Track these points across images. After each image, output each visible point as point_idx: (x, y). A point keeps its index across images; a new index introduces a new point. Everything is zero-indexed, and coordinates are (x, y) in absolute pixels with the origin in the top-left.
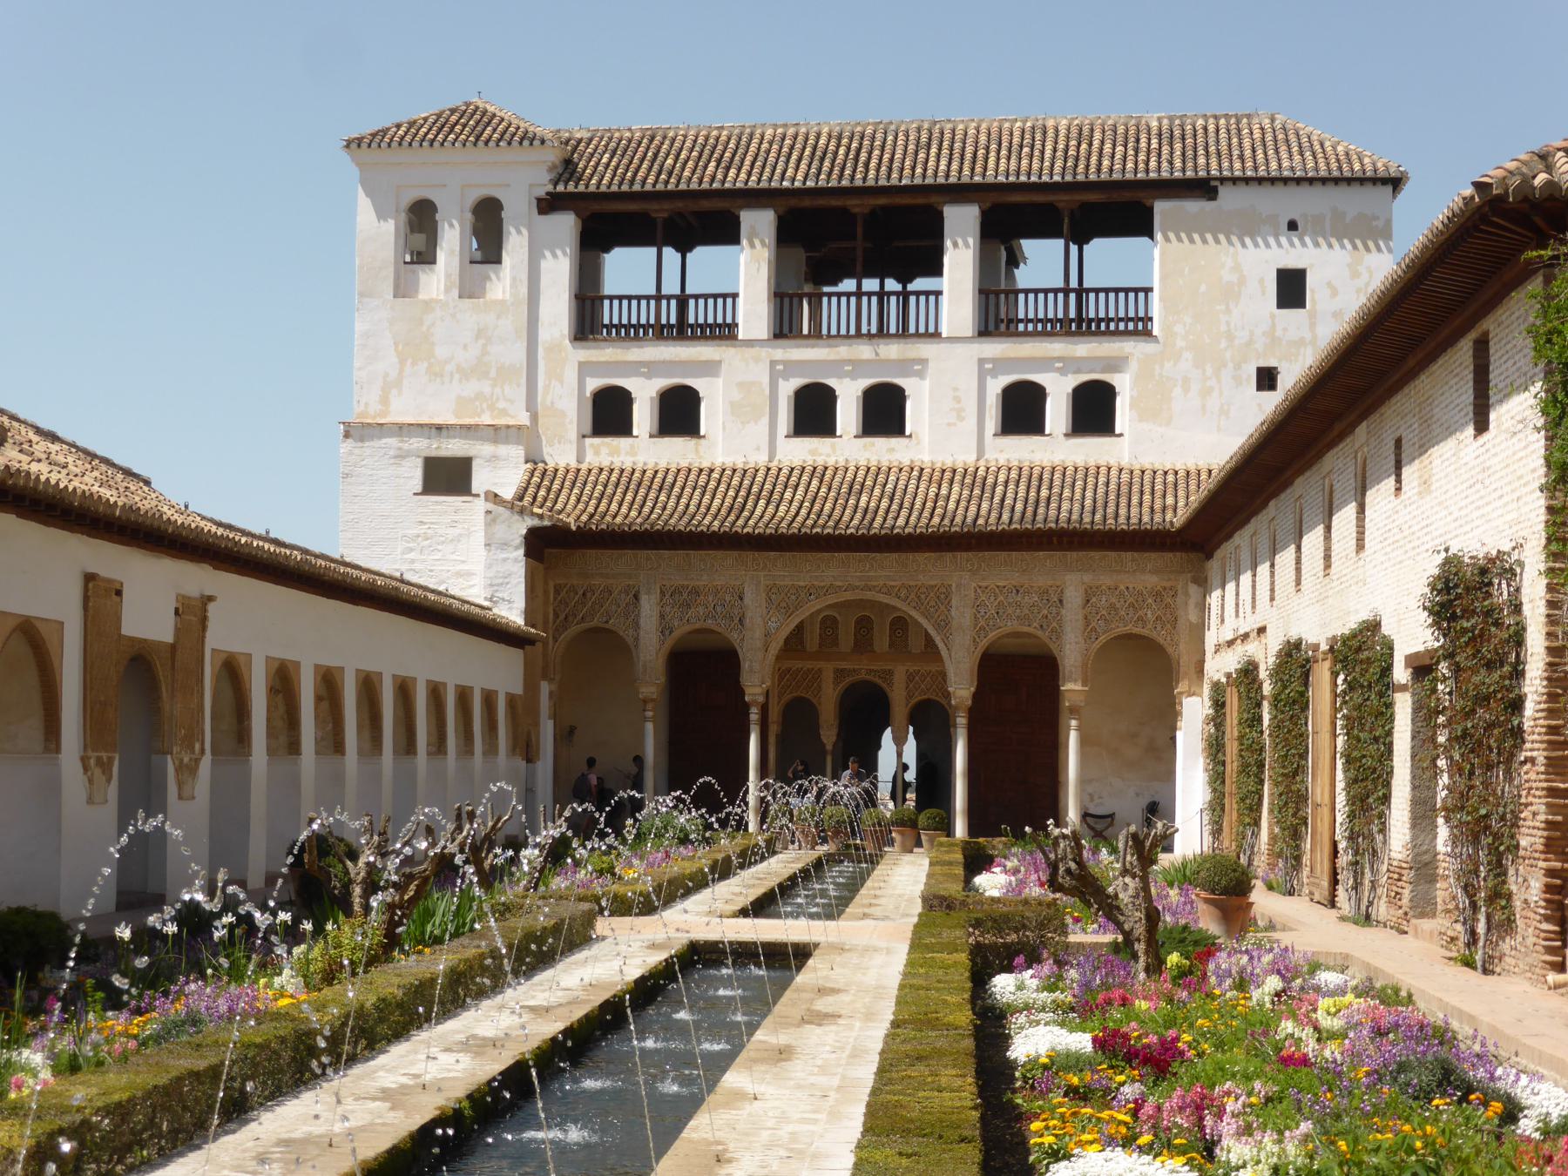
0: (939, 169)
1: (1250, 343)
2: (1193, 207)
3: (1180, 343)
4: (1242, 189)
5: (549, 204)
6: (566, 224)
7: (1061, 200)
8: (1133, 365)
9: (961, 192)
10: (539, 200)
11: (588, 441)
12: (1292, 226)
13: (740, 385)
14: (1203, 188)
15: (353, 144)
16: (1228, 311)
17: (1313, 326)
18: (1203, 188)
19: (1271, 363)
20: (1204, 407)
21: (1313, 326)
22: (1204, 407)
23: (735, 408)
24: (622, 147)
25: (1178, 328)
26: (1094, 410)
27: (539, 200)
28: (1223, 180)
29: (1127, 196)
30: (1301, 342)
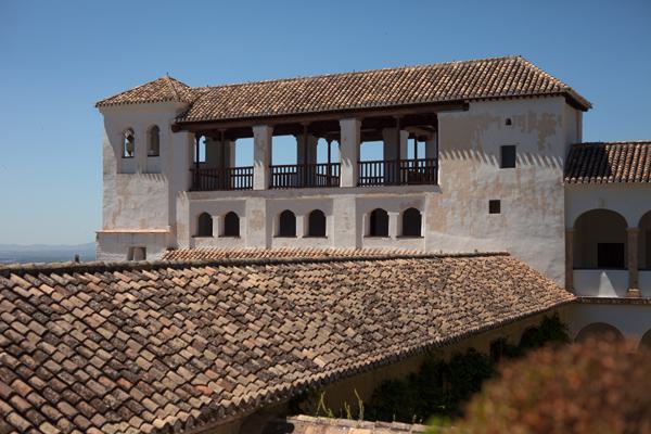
0: (343, 101)
1: (485, 188)
2: (457, 115)
3: (450, 188)
4: (481, 103)
5: (177, 128)
6: (184, 135)
7: (395, 114)
8: (427, 202)
9: (348, 113)
10: (173, 126)
11: (197, 239)
12: (509, 122)
13: (254, 212)
14: (461, 104)
15: (99, 105)
16: (474, 169)
17: (518, 177)
18: (461, 104)
19: (497, 198)
20: (462, 223)
21: (518, 177)
22: (462, 223)
23: (252, 223)
24: (216, 94)
25: (450, 181)
26: (411, 226)
27: (173, 126)
28: (471, 100)
29: (426, 110)
30: (512, 187)
